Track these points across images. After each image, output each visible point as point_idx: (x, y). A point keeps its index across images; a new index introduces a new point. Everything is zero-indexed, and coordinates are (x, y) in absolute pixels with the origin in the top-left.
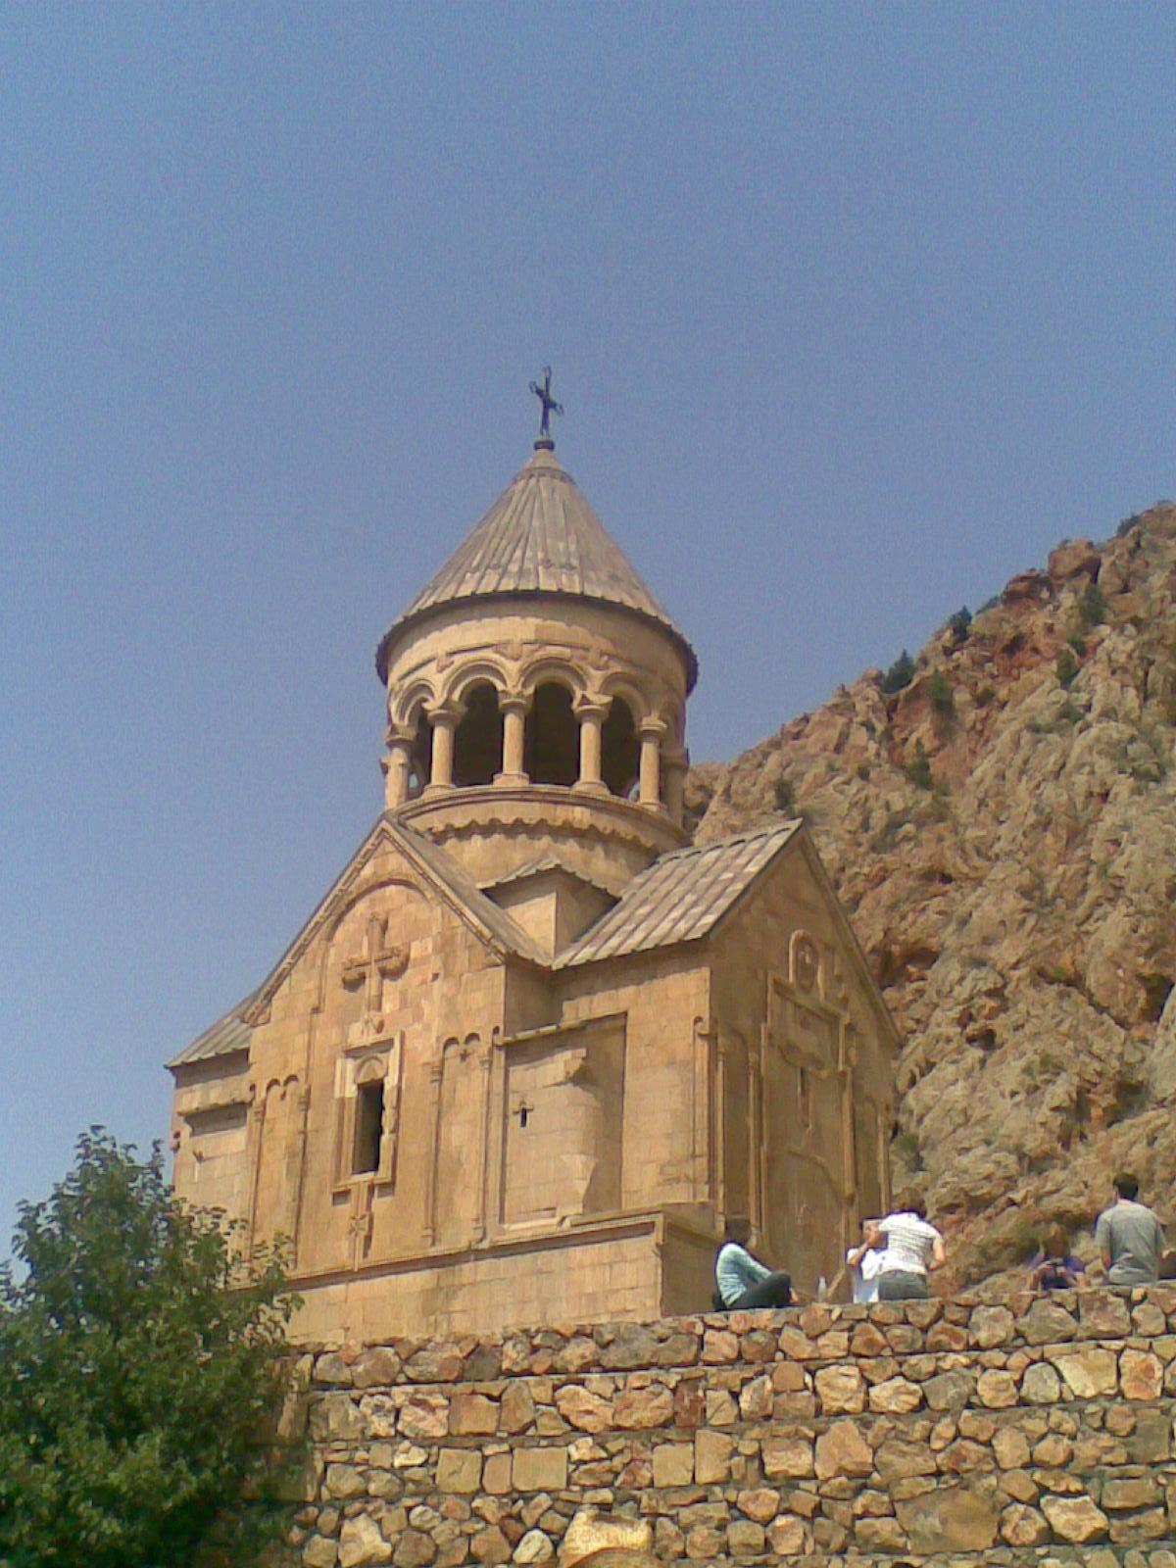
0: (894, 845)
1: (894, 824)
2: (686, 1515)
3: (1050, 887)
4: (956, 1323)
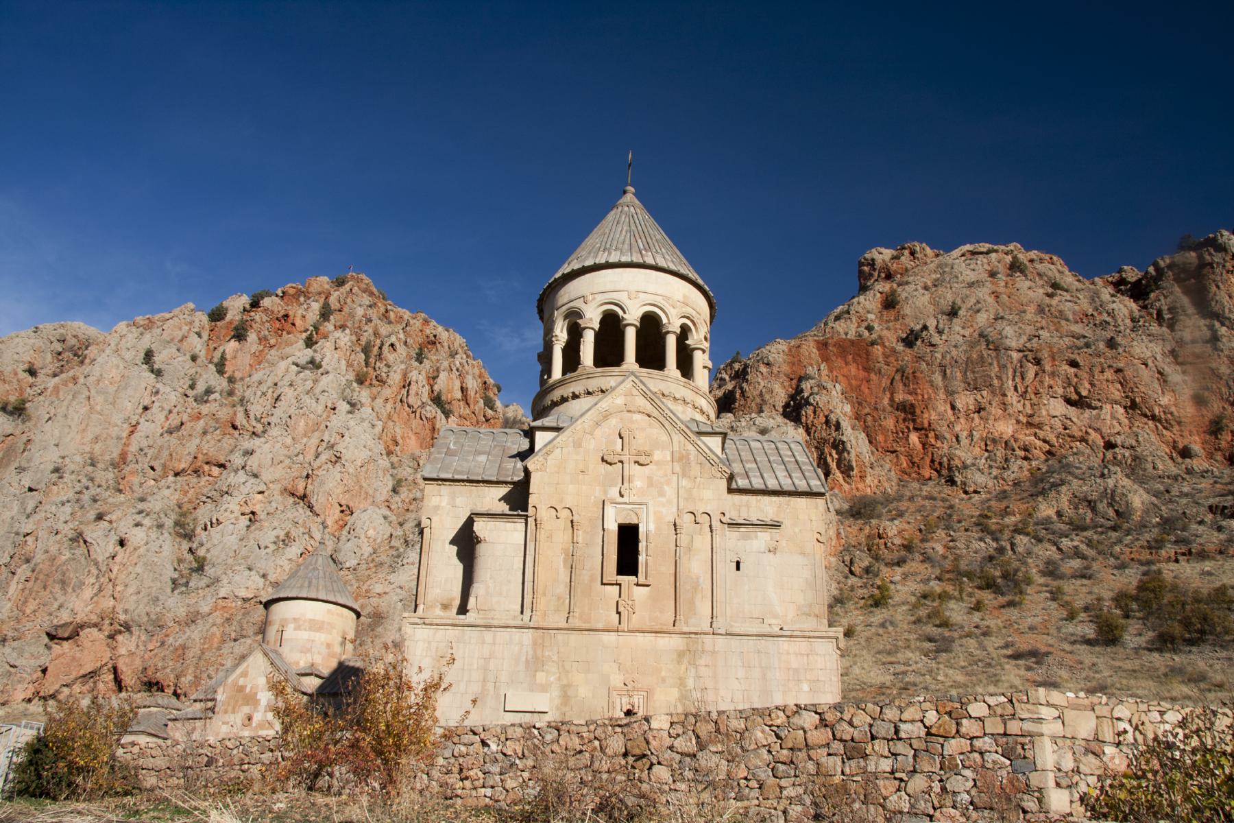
0: (206, 402)
1: (209, 391)
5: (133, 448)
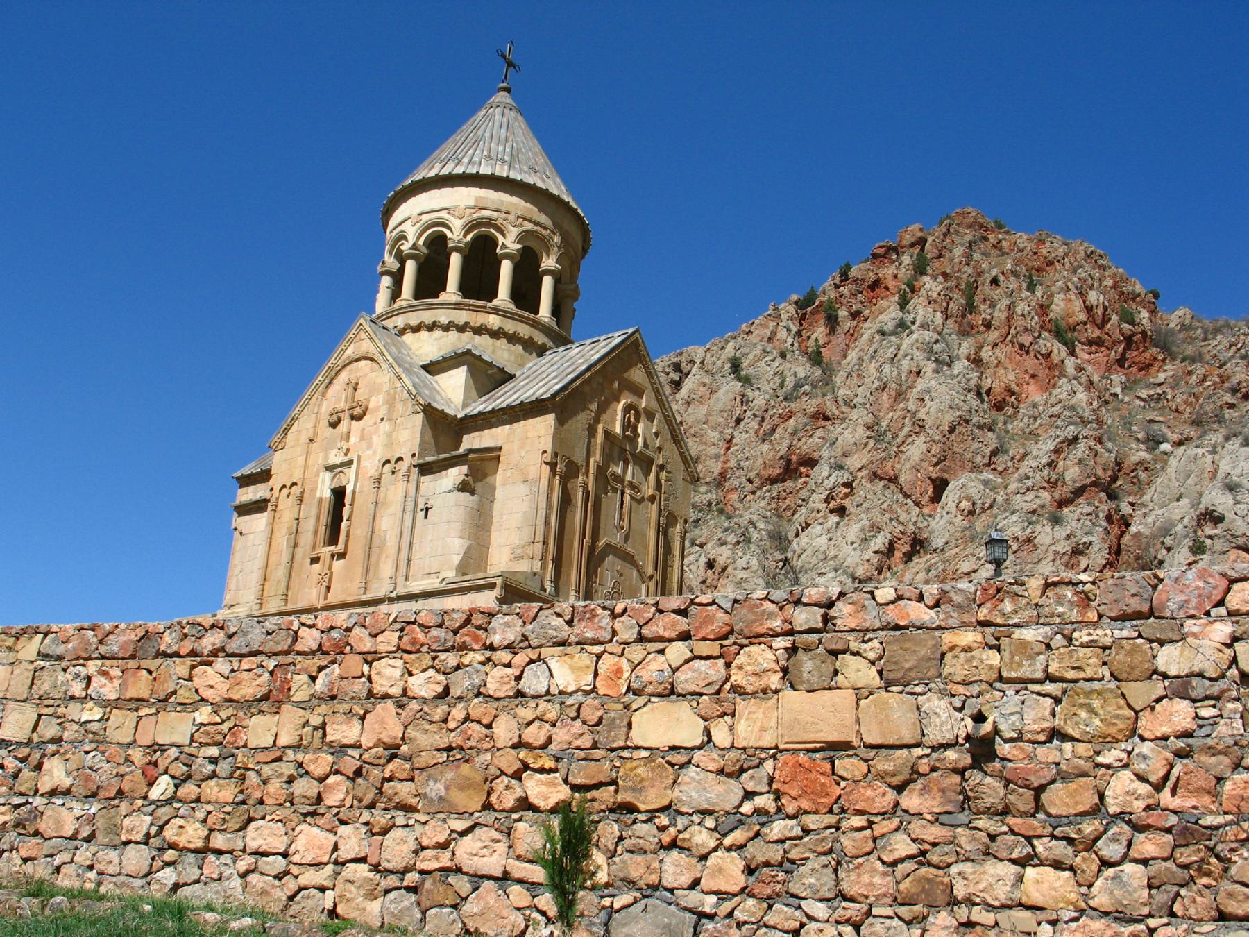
1: (798, 386)
2: (267, 770)
3: (884, 424)
4: (479, 628)
5: (732, 464)
